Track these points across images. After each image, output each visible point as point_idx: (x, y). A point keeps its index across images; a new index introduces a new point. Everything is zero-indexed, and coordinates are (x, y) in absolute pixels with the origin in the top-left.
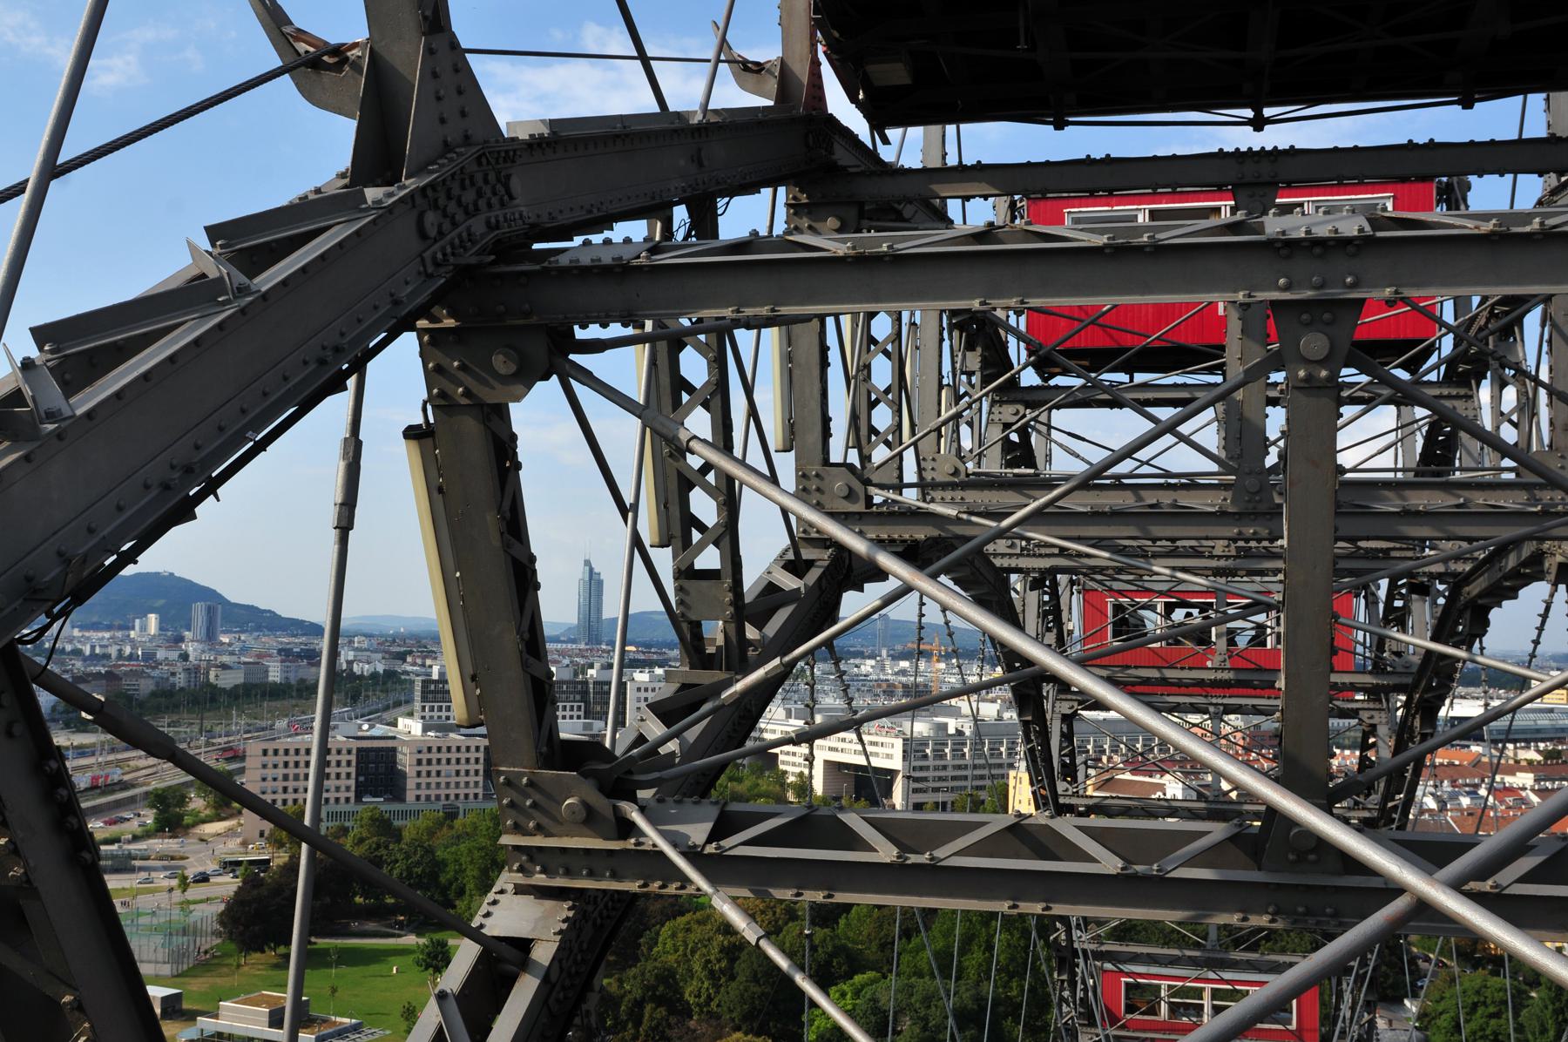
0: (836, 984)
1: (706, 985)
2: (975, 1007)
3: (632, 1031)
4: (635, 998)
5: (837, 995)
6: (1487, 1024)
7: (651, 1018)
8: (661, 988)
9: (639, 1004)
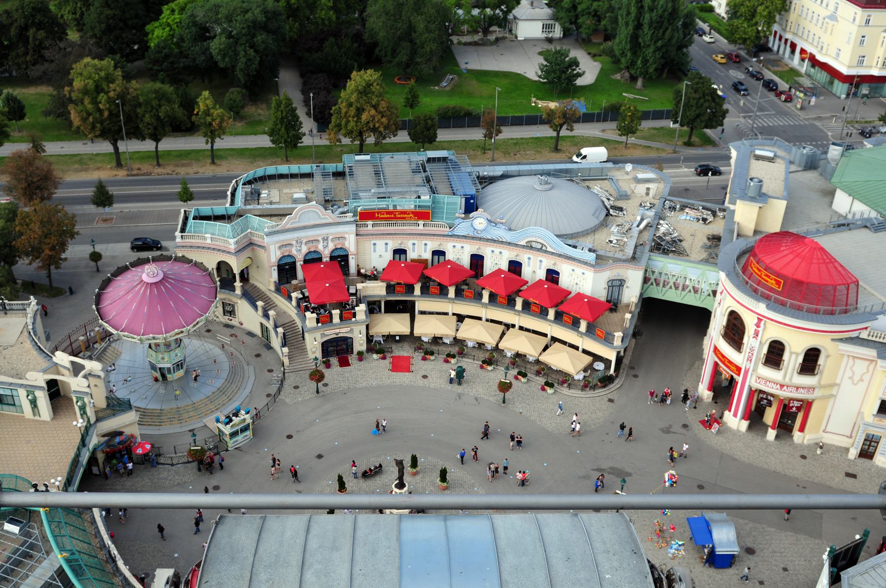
0: (167, 4)
1: (79, 5)
2: (264, 19)
3: (23, 49)
4: (21, 26)
5: (168, 12)
6: (591, 5)
7: (35, 39)
8: (38, 17)
9: (24, 29)
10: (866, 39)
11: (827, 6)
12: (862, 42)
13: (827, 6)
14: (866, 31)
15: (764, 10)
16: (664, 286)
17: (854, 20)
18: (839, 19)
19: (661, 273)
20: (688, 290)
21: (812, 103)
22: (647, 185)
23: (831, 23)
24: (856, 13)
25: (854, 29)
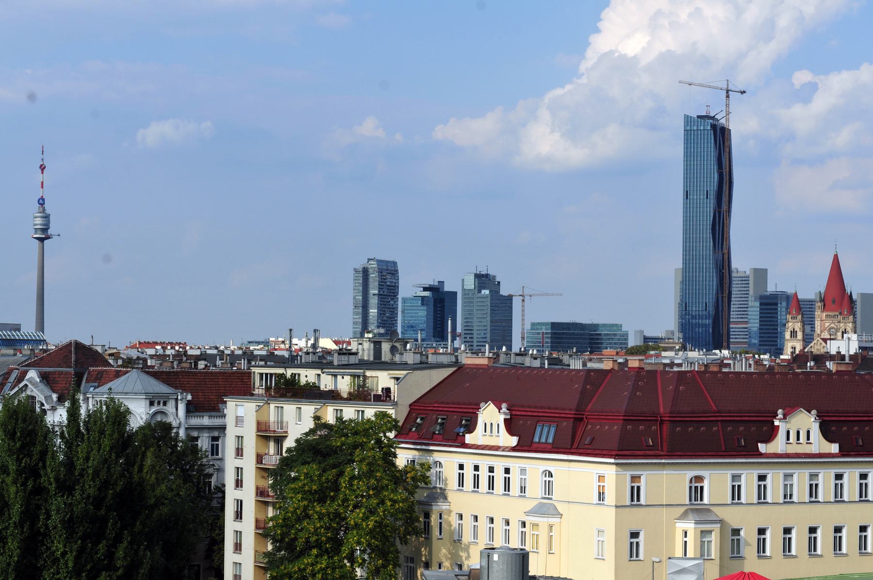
10: (641, 539)
11: (523, 489)
12: (634, 551)
13: (523, 489)
14: (636, 518)
15: (366, 518)
17: (601, 496)
18: (561, 508)
23: (543, 522)
24: (601, 478)
25: (607, 517)
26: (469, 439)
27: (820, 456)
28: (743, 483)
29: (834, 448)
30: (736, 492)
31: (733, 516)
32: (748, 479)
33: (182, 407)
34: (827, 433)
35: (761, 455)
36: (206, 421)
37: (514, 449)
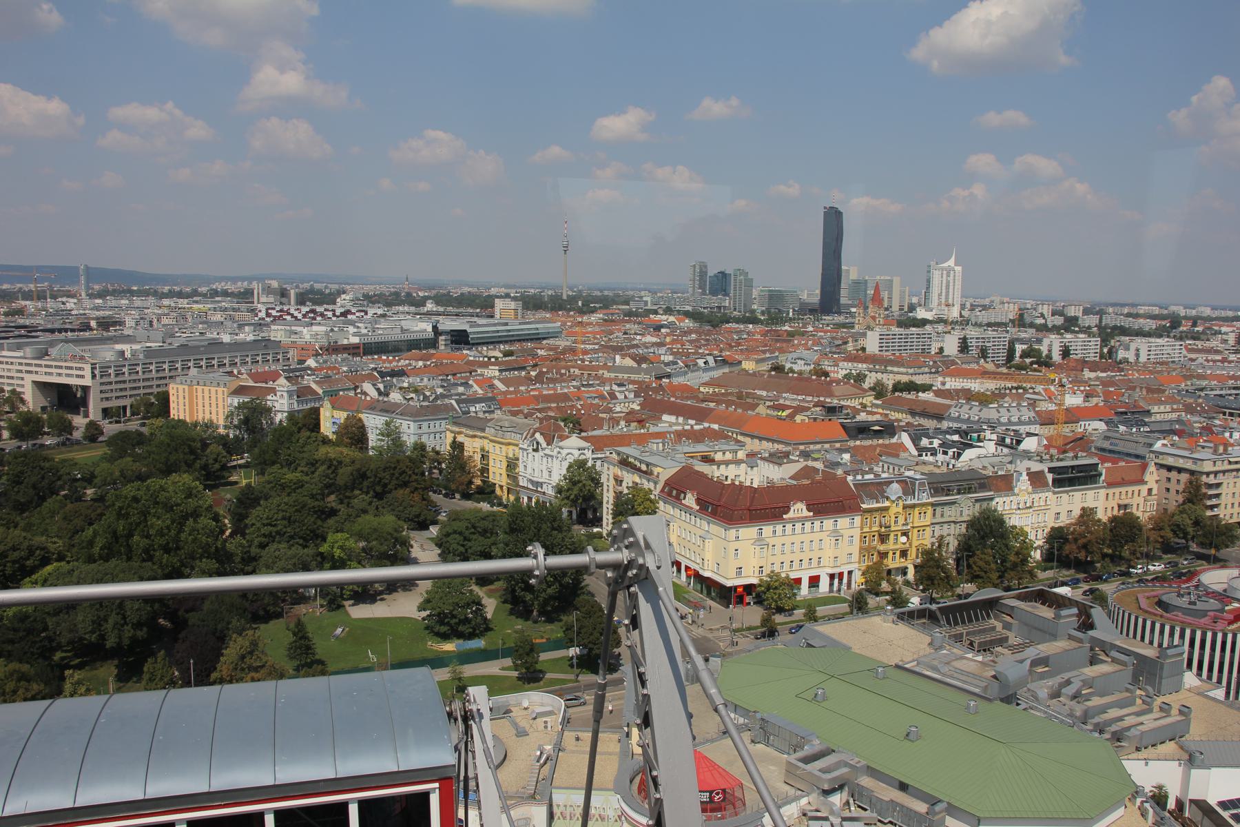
16: (571, 819)
19: (565, 806)
20: (595, 819)
21: (701, 616)
22: (544, 719)
26: (683, 502)
27: (806, 517)
28: (777, 529)
29: (811, 514)
30: (775, 532)
31: (771, 541)
32: (779, 528)
33: (590, 451)
34: (809, 510)
35: (784, 519)
36: (599, 456)
37: (697, 511)
